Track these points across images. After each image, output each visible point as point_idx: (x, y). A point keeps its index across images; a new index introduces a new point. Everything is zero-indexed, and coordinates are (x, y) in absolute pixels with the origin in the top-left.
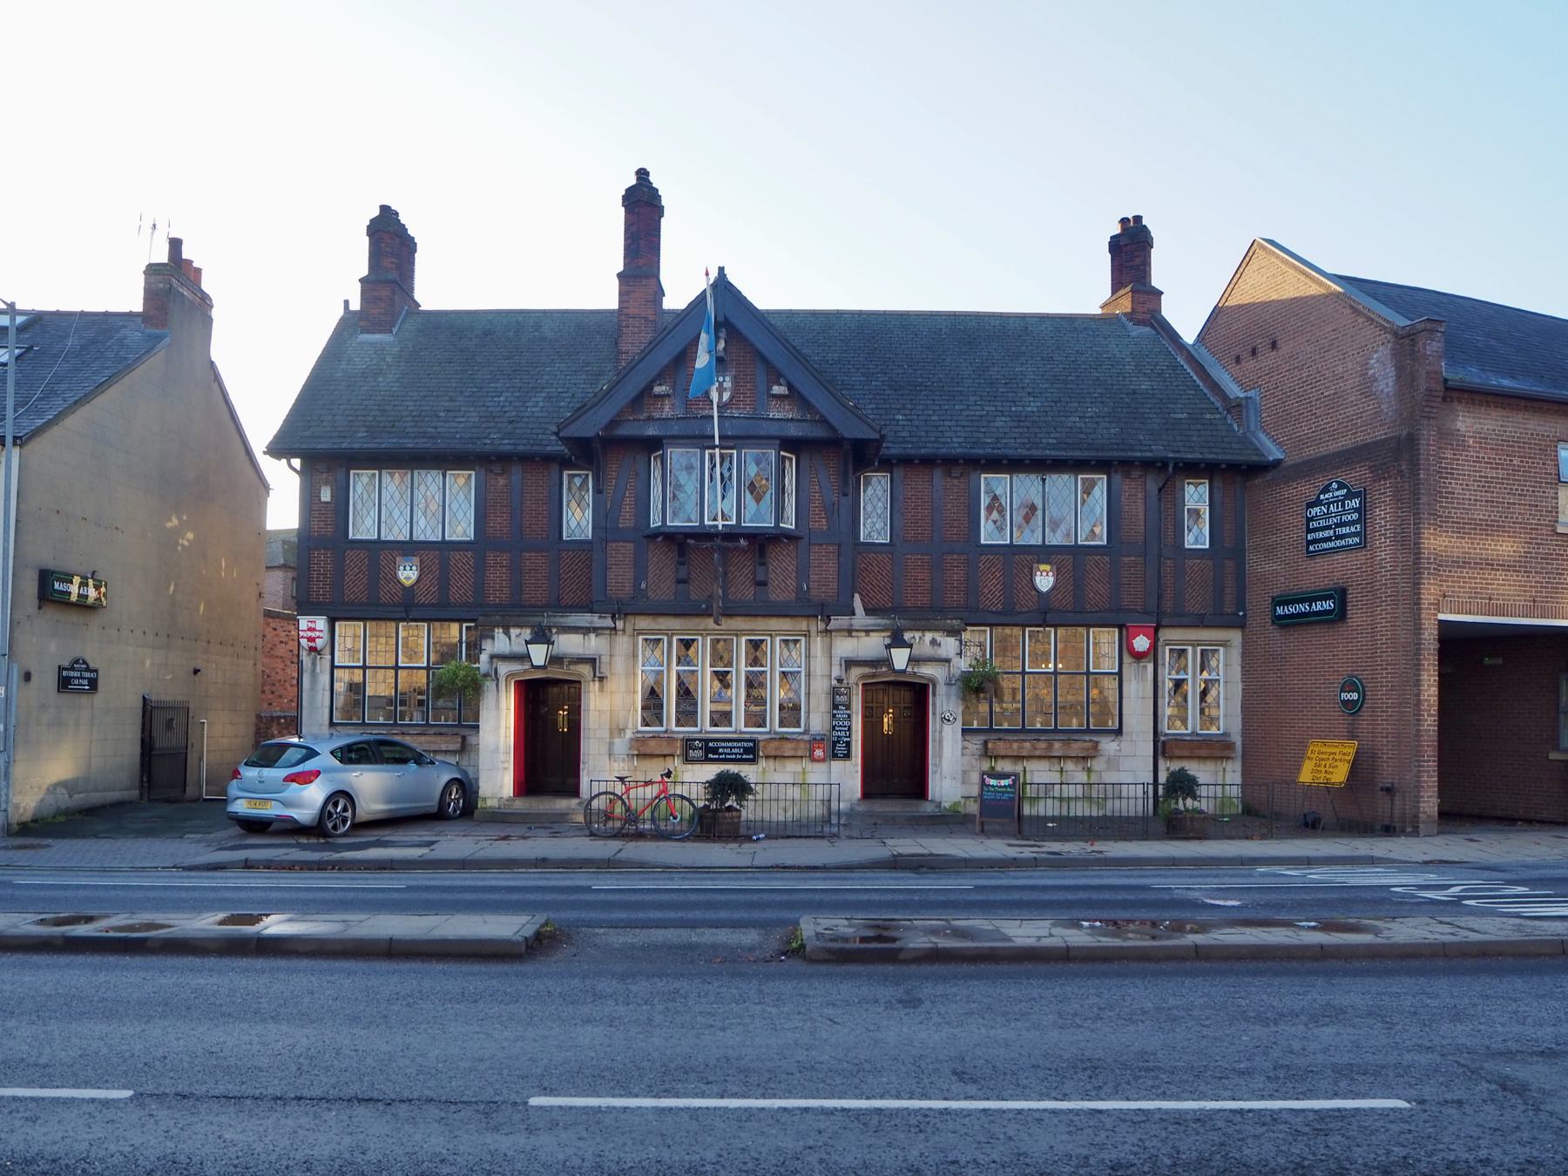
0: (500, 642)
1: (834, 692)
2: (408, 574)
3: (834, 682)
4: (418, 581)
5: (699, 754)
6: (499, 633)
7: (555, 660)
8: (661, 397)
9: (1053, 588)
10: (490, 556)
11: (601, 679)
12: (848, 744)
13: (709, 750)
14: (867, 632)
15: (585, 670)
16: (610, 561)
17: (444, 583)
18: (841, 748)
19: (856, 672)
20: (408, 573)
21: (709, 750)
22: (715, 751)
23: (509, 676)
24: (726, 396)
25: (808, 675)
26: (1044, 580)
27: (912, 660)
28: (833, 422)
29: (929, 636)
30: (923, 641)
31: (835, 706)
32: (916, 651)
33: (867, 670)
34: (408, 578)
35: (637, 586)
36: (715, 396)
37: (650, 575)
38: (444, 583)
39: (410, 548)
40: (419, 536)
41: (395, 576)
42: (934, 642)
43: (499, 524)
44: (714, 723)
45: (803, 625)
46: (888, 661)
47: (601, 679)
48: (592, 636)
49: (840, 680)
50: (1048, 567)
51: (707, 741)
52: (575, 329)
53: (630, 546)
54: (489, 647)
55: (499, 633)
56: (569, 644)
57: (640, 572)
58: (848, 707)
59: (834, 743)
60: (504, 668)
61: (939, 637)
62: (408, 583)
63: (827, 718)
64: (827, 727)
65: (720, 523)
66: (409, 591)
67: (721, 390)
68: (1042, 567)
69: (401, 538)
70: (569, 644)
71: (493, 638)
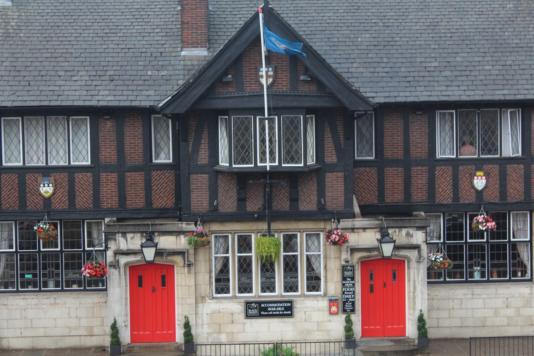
0: (122, 243)
1: (344, 269)
2: (47, 190)
3: (343, 263)
4: (53, 194)
5: (255, 312)
6: (119, 237)
7: (159, 253)
8: (228, 83)
9: (486, 187)
10: (103, 176)
11: (189, 265)
12: (353, 303)
13: (261, 309)
14: (364, 229)
15: (178, 259)
16: (193, 186)
17: (72, 195)
18: (348, 306)
19: (358, 255)
20: (47, 189)
21: (261, 309)
22: (265, 309)
23: (126, 265)
24: (270, 80)
25: (326, 258)
26: (480, 183)
27: (397, 248)
28: (340, 96)
29: (404, 231)
30: (400, 236)
31: (344, 279)
32: (397, 243)
33: (365, 254)
34: (47, 192)
35: (211, 203)
36: (263, 81)
37: (220, 195)
38: (72, 195)
39: (46, 171)
40: (53, 163)
41: (38, 189)
42: (408, 234)
43: (108, 154)
44: (263, 291)
45: (321, 225)
46: (378, 249)
47: (189, 265)
48: (182, 237)
49: (347, 262)
50: (482, 173)
51: (260, 303)
52: (273, 221)
53: (206, 176)
54: (112, 246)
55: (119, 237)
56: (166, 242)
57: (213, 194)
58: (353, 278)
59: (344, 303)
60: (123, 260)
61: (411, 231)
62: (47, 195)
63: (339, 285)
64: (339, 291)
65: (268, 165)
66: (47, 201)
67: (268, 77)
68: (478, 173)
69: (40, 164)
70: (166, 242)
71: (115, 240)
